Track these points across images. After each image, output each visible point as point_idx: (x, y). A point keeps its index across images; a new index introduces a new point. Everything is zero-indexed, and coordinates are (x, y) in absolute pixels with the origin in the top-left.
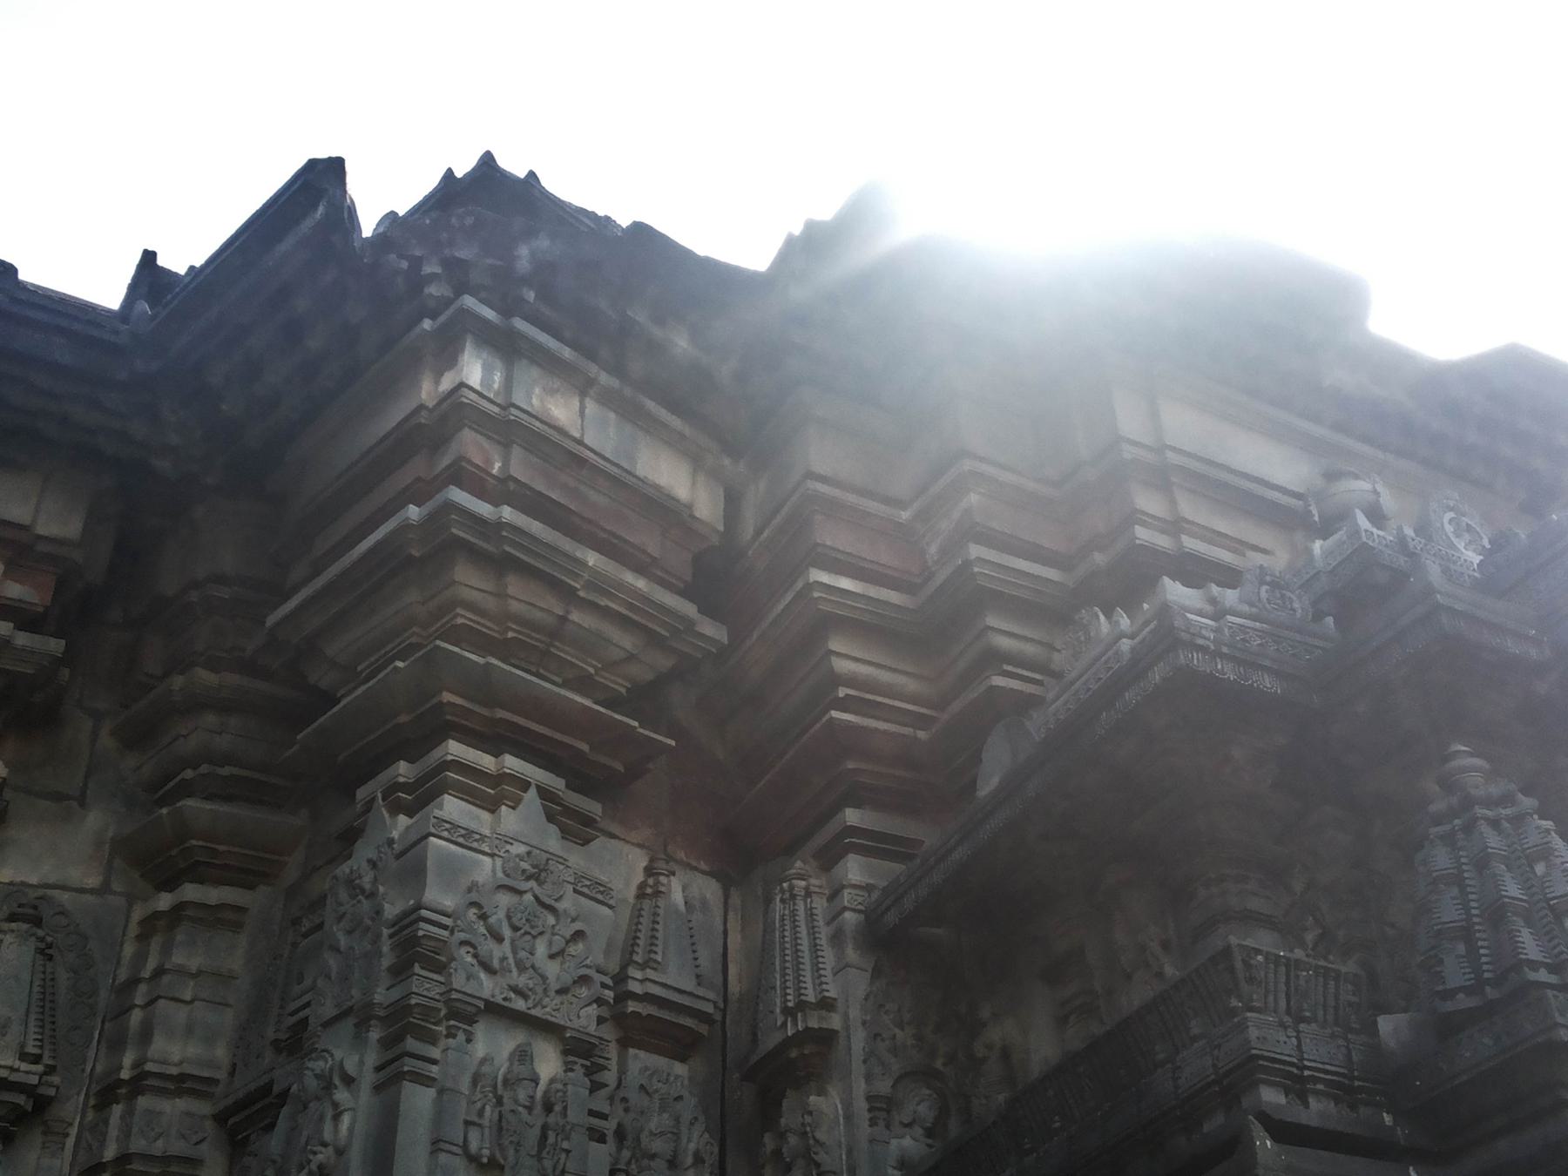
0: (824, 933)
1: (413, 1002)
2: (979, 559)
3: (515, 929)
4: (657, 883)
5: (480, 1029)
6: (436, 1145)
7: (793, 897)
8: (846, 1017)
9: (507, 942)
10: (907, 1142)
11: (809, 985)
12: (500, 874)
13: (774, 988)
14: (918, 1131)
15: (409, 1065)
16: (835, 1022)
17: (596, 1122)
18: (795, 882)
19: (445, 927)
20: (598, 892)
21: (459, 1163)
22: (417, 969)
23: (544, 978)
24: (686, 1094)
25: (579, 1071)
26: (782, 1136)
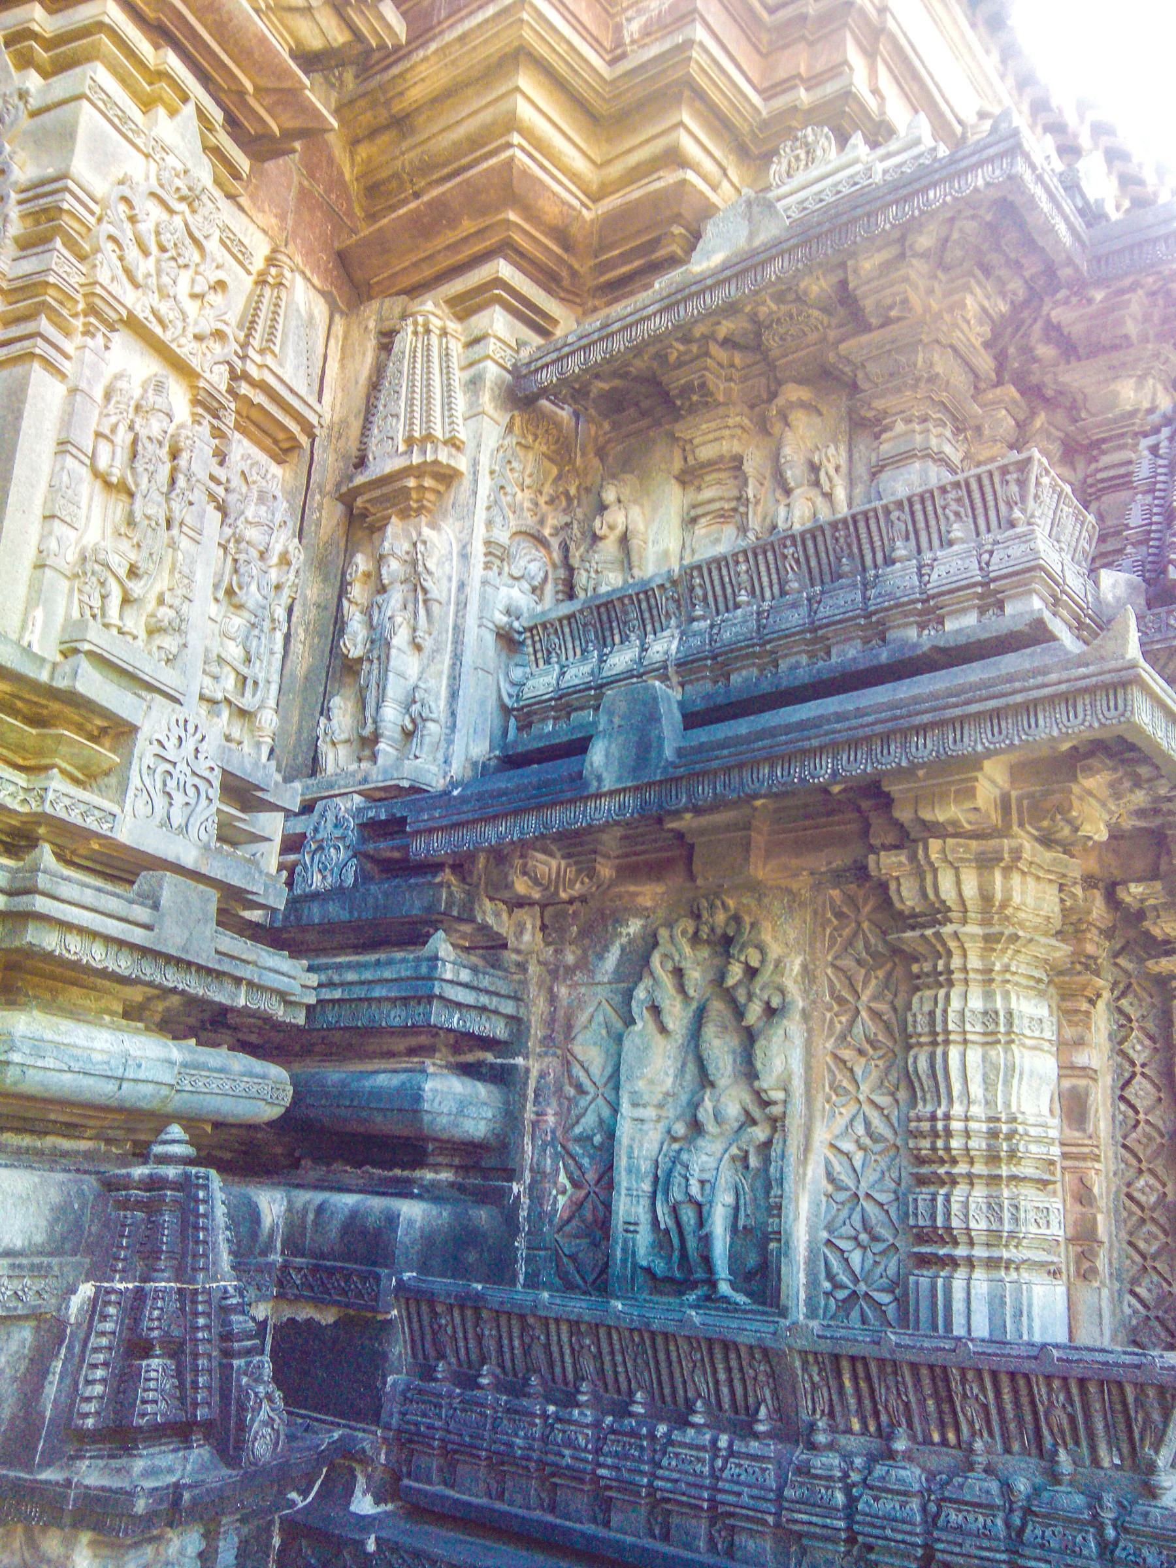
0: (459, 377)
1: (51, 280)
2: (701, 44)
3: (163, 249)
4: (281, 275)
5: (117, 339)
6: (64, 446)
7: (428, 331)
8: (475, 463)
9: (152, 259)
10: (515, 593)
11: (439, 421)
12: (153, 181)
13: (397, 416)
14: (526, 586)
15: (41, 347)
16: (462, 463)
17: (212, 485)
18: (432, 319)
19: (92, 213)
20: (238, 252)
21: (85, 472)
22: (58, 243)
23: (183, 313)
24: (279, 494)
25: (205, 430)
26: (380, 560)
